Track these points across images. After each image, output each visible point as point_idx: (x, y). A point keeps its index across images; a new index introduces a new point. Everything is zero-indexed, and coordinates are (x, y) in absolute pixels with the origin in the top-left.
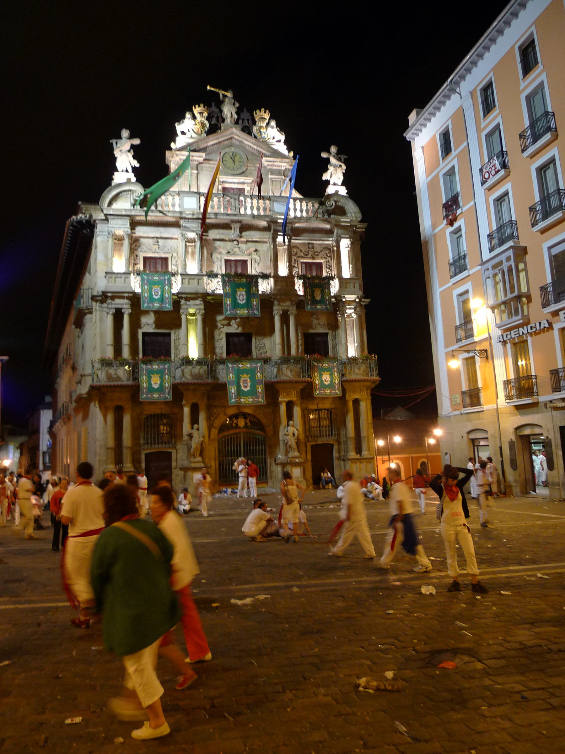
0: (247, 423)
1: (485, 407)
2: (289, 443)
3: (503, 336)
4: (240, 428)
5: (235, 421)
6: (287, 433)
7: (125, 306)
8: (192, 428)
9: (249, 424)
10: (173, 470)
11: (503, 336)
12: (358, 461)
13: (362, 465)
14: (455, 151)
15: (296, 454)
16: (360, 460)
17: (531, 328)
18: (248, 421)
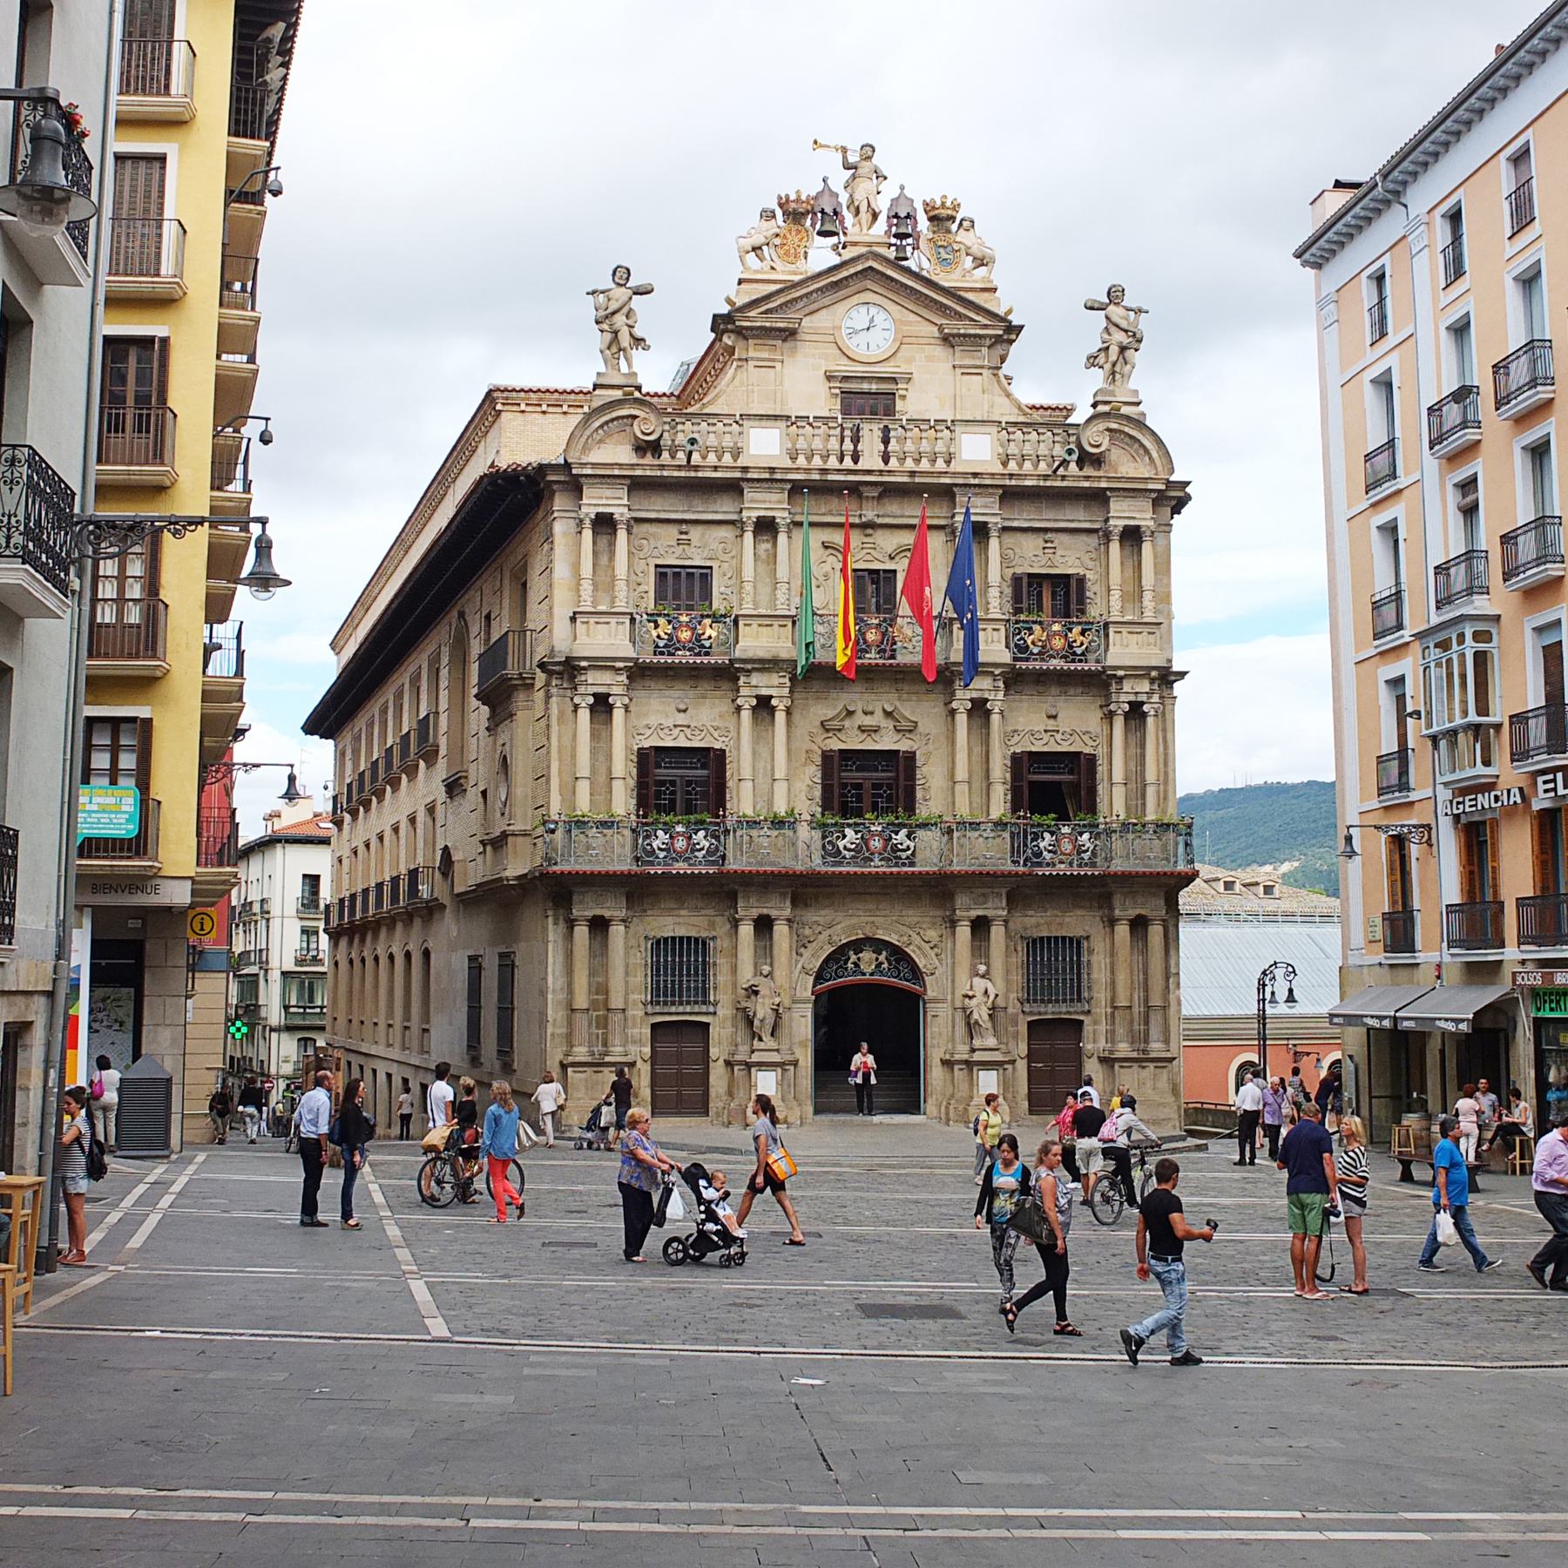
0: (882, 963)
1: (1421, 957)
2: (976, 1016)
3: (1451, 802)
4: (864, 974)
5: (853, 958)
6: (970, 993)
7: (615, 690)
8: (757, 972)
9: (885, 965)
10: (711, 1064)
11: (1451, 802)
12: (1136, 1065)
13: (1145, 1073)
14: (1395, 334)
15: (991, 1042)
16: (1142, 1061)
17: (1497, 799)
18: (882, 958)
